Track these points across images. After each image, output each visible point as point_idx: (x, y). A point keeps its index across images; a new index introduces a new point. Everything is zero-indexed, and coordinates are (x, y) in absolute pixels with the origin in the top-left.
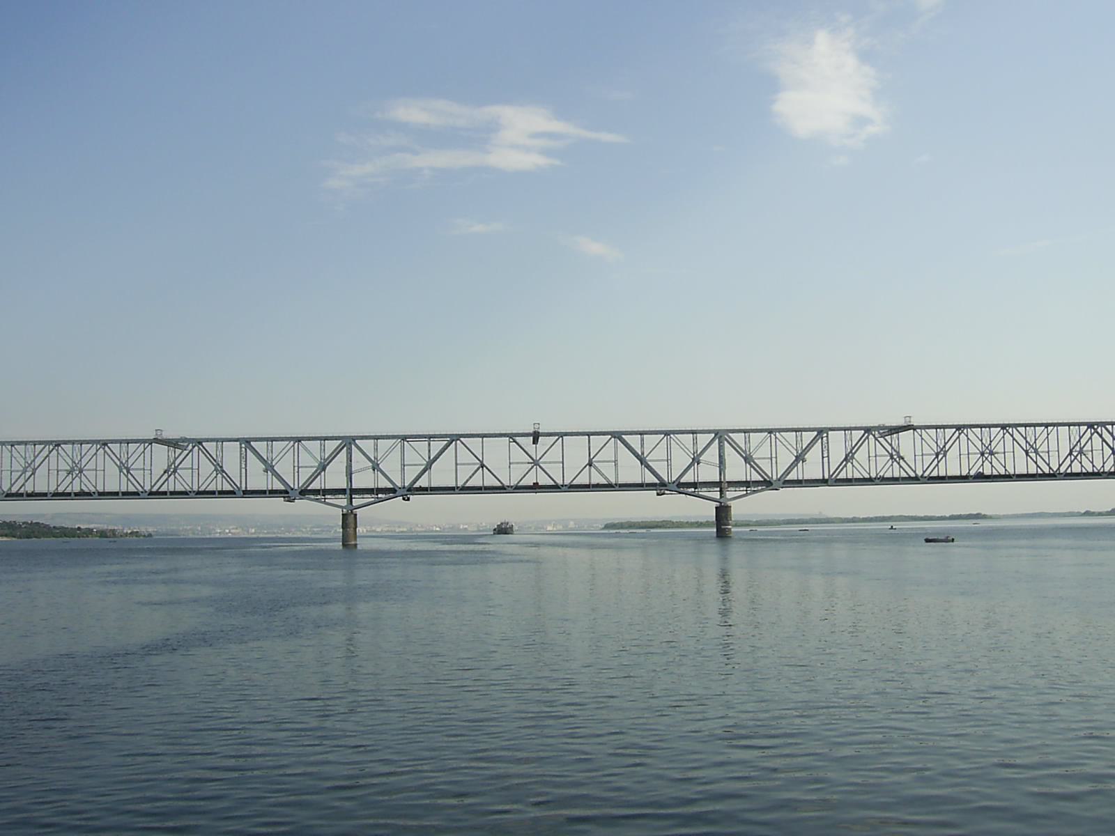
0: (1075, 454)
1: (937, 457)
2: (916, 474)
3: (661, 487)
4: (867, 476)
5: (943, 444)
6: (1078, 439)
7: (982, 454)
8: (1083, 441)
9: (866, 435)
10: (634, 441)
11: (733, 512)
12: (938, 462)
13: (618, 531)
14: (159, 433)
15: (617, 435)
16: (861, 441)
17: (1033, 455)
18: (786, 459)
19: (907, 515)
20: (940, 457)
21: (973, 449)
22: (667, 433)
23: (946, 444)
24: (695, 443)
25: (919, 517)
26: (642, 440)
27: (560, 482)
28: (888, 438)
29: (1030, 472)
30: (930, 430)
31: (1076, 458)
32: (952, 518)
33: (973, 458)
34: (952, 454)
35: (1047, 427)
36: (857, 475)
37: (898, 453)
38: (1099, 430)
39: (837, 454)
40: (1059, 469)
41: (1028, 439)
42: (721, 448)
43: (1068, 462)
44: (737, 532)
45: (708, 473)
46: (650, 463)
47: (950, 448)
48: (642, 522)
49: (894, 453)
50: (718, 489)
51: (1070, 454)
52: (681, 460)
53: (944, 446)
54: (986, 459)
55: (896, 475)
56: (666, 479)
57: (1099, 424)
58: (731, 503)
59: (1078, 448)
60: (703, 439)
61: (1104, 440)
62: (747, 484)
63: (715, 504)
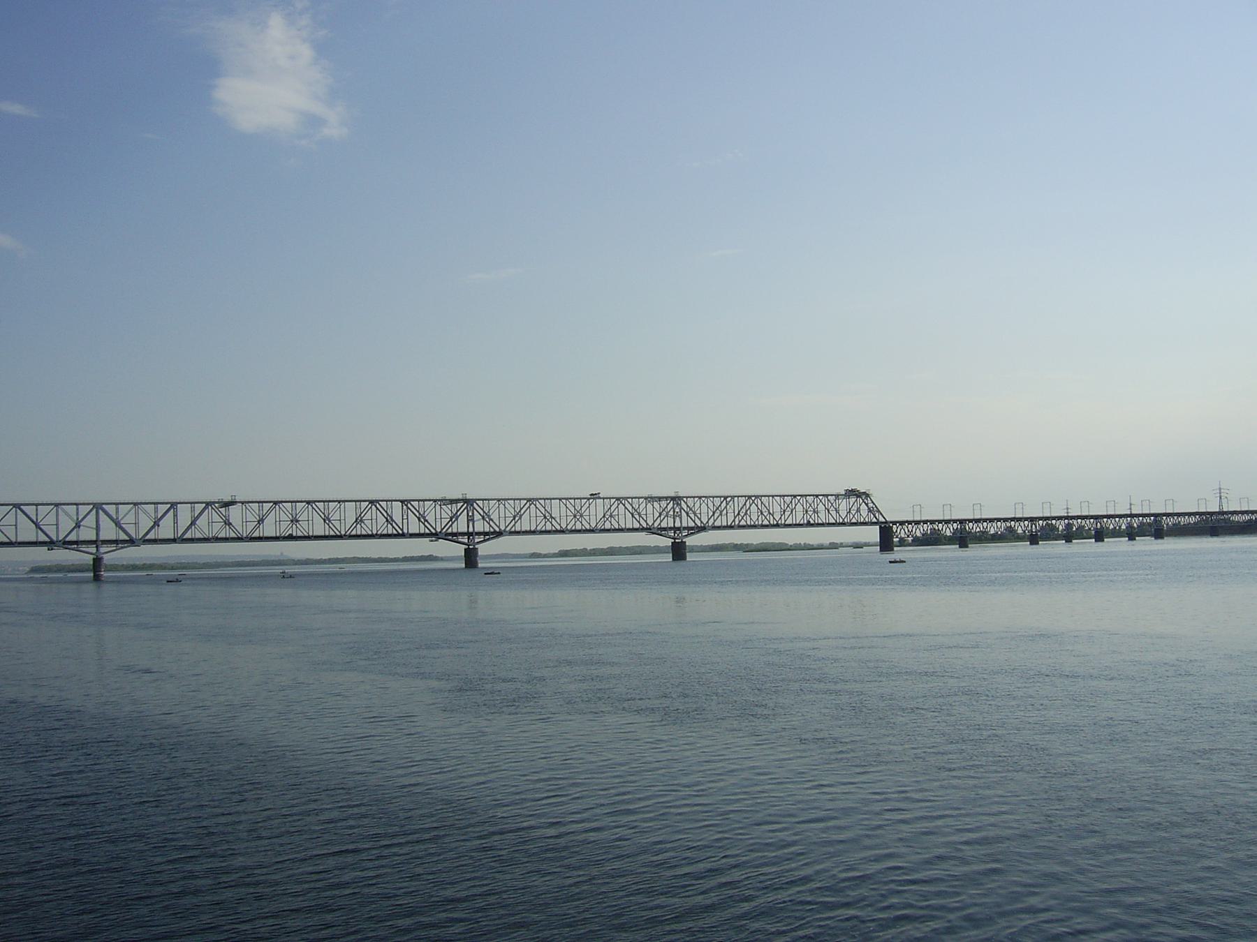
0: (853, 512)
1: (514, 519)
2: (500, 529)
3: (51, 544)
4: (370, 533)
5: (519, 509)
6: (609, 506)
7: (575, 516)
8: (612, 509)
9: (370, 505)
10: (30, 510)
11: (687, 544)
12: (515, 523)
13: (45, 575)
14: (233, 498)
15: (17, 506)
16: (270, 511)
17: (637, 517)
18: (146, 523)
19: (361, 556)
20: (517, 519)
21: (569, 513)
22: (135, 504)
23: (521, 509)
24: (156, 511)
25: (373, 559)
26: (77, 509)
27: (14, 540)
28: (449, 506)
29: (635, 527)
30: (320, 503)
31: (742, 518)
32: (406, 559)
33: (539, 519)
34: (526, 517)
35: (339, 503)
36: (364, 533)
37: (391, 518)
38: (623, 502)
39: (184, 520)
40: (653, 524)
41: (546, 508)
42: (97, 513)
43: (658, 521)
44: (107, 577)
45: (87, 534)
46: (41, 526)
47: (524, 513)
48: (73, 565)
49: (547, 515)
50: (95, 546)
51: (604, 517)
52: (66, 524)
53: (520, 511)
54: (578, 519)
55: (390, 532)
56: (134, 537)
57: (623, 498)
58: (104, 556)
59: (609, 513)
60: (84, 510)
61: (626, 508)
62: (116, 542)
63: (92, 557)
